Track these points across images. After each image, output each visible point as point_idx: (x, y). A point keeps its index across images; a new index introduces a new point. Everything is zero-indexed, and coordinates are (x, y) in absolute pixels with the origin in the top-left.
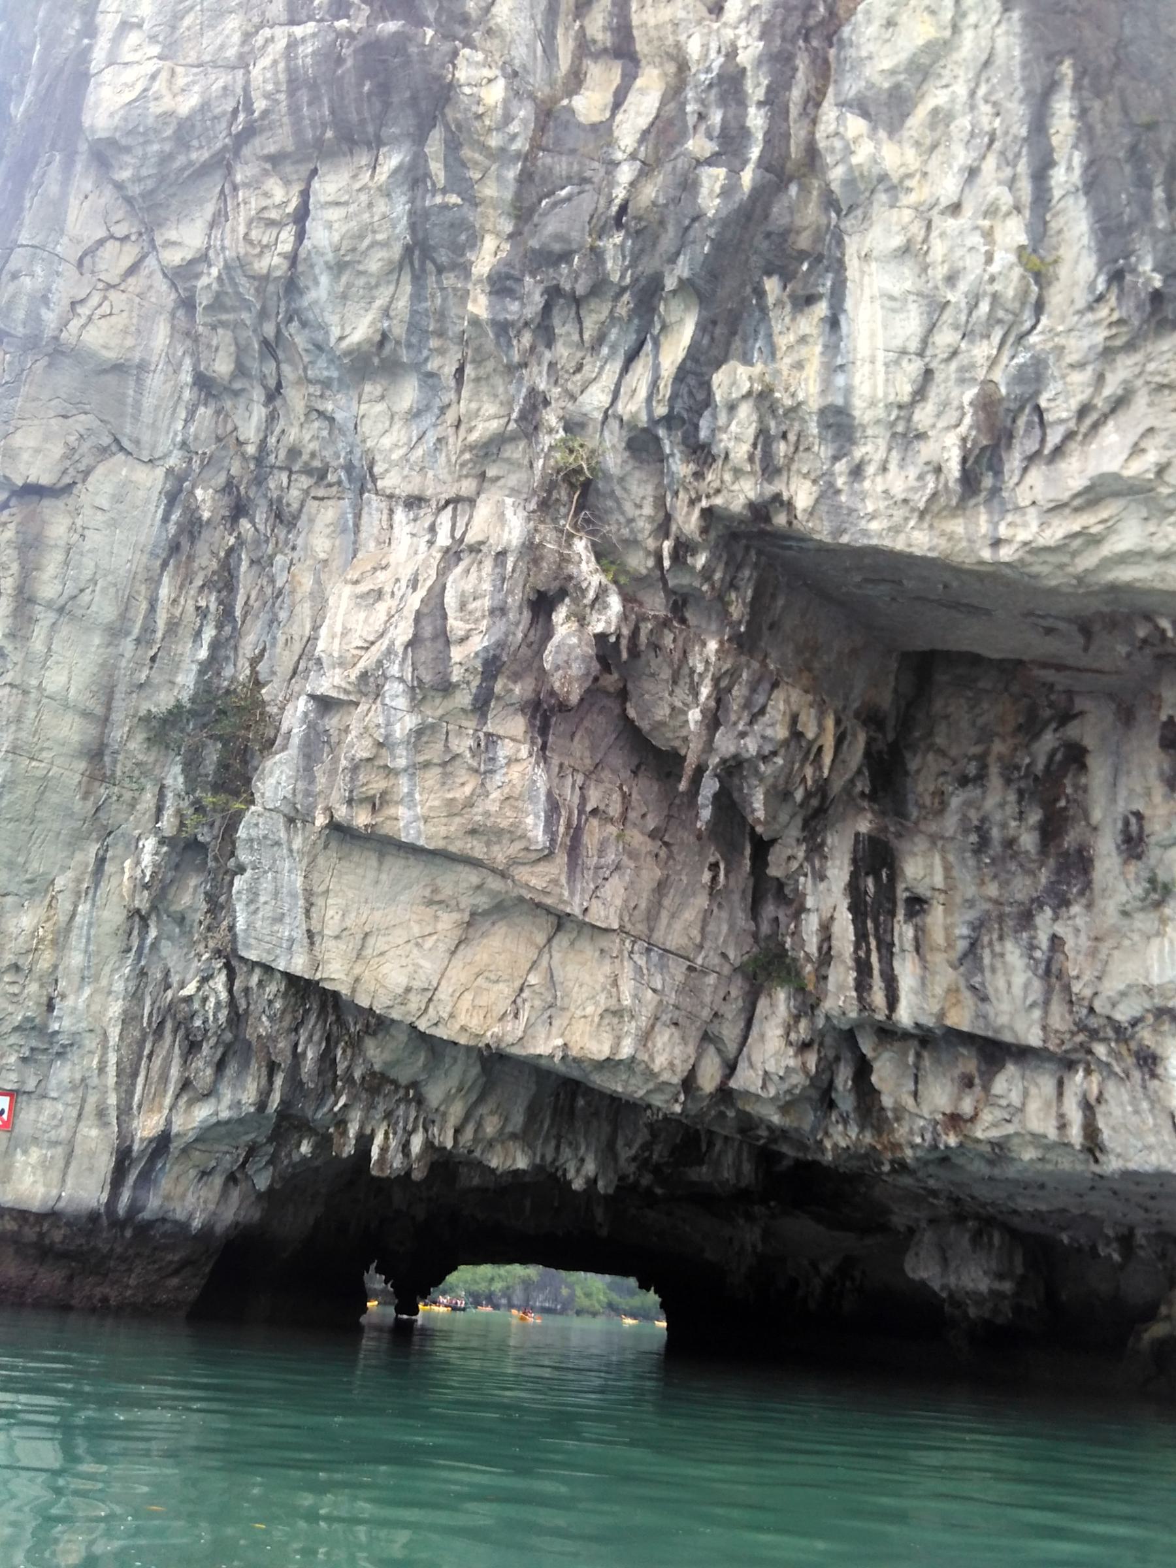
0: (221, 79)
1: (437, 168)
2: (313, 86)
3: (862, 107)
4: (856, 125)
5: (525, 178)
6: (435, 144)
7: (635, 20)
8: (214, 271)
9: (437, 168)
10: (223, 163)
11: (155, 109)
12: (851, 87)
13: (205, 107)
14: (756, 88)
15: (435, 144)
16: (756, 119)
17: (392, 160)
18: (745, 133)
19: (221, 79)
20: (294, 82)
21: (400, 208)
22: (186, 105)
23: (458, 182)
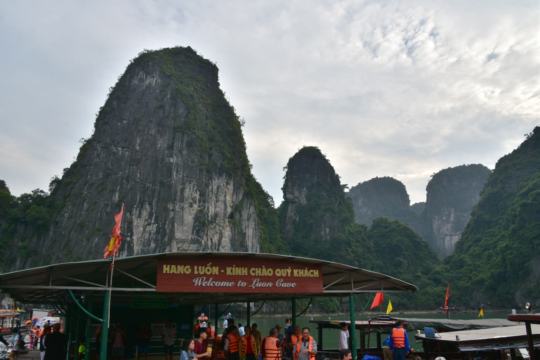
0: (186, 237)
1: (199, 246)
2: (193, 240)
3: (222, 247)
4: (221, 248)
5: (204, 248)
6: (199, 245)
7: (208, 234)
8: (182, 248)
9: (199, 246)
10: (184, 242)
11: (181, 238)
12: (221, 246)
13: (185, 239)
14: (217, 245)
15: (199, 245)
16: (217, 247)
17: (197, 245)
18: (216, 248)
19: (186, 237)
20: (192, 239)
21: (196, 248)
22: (184, 238)
23: (200, 247)
